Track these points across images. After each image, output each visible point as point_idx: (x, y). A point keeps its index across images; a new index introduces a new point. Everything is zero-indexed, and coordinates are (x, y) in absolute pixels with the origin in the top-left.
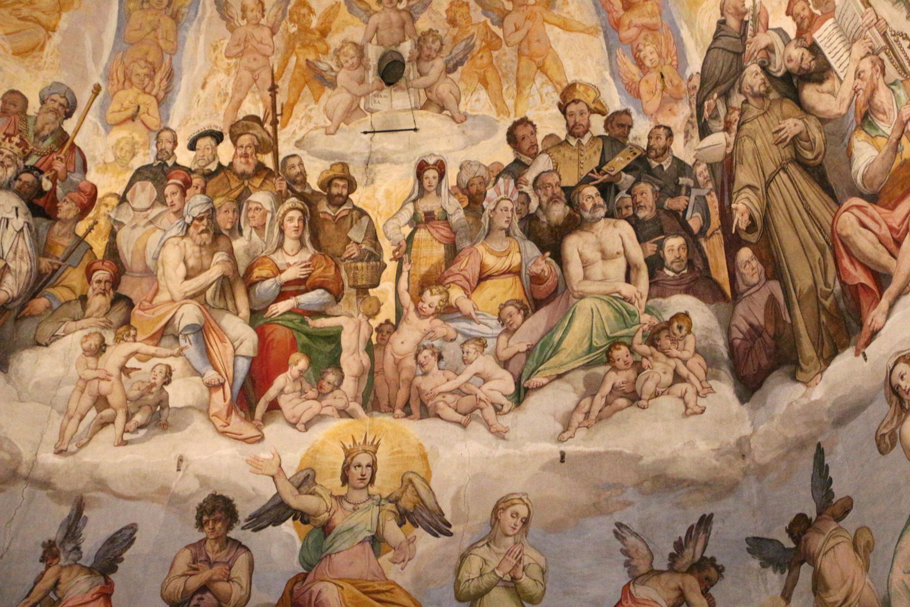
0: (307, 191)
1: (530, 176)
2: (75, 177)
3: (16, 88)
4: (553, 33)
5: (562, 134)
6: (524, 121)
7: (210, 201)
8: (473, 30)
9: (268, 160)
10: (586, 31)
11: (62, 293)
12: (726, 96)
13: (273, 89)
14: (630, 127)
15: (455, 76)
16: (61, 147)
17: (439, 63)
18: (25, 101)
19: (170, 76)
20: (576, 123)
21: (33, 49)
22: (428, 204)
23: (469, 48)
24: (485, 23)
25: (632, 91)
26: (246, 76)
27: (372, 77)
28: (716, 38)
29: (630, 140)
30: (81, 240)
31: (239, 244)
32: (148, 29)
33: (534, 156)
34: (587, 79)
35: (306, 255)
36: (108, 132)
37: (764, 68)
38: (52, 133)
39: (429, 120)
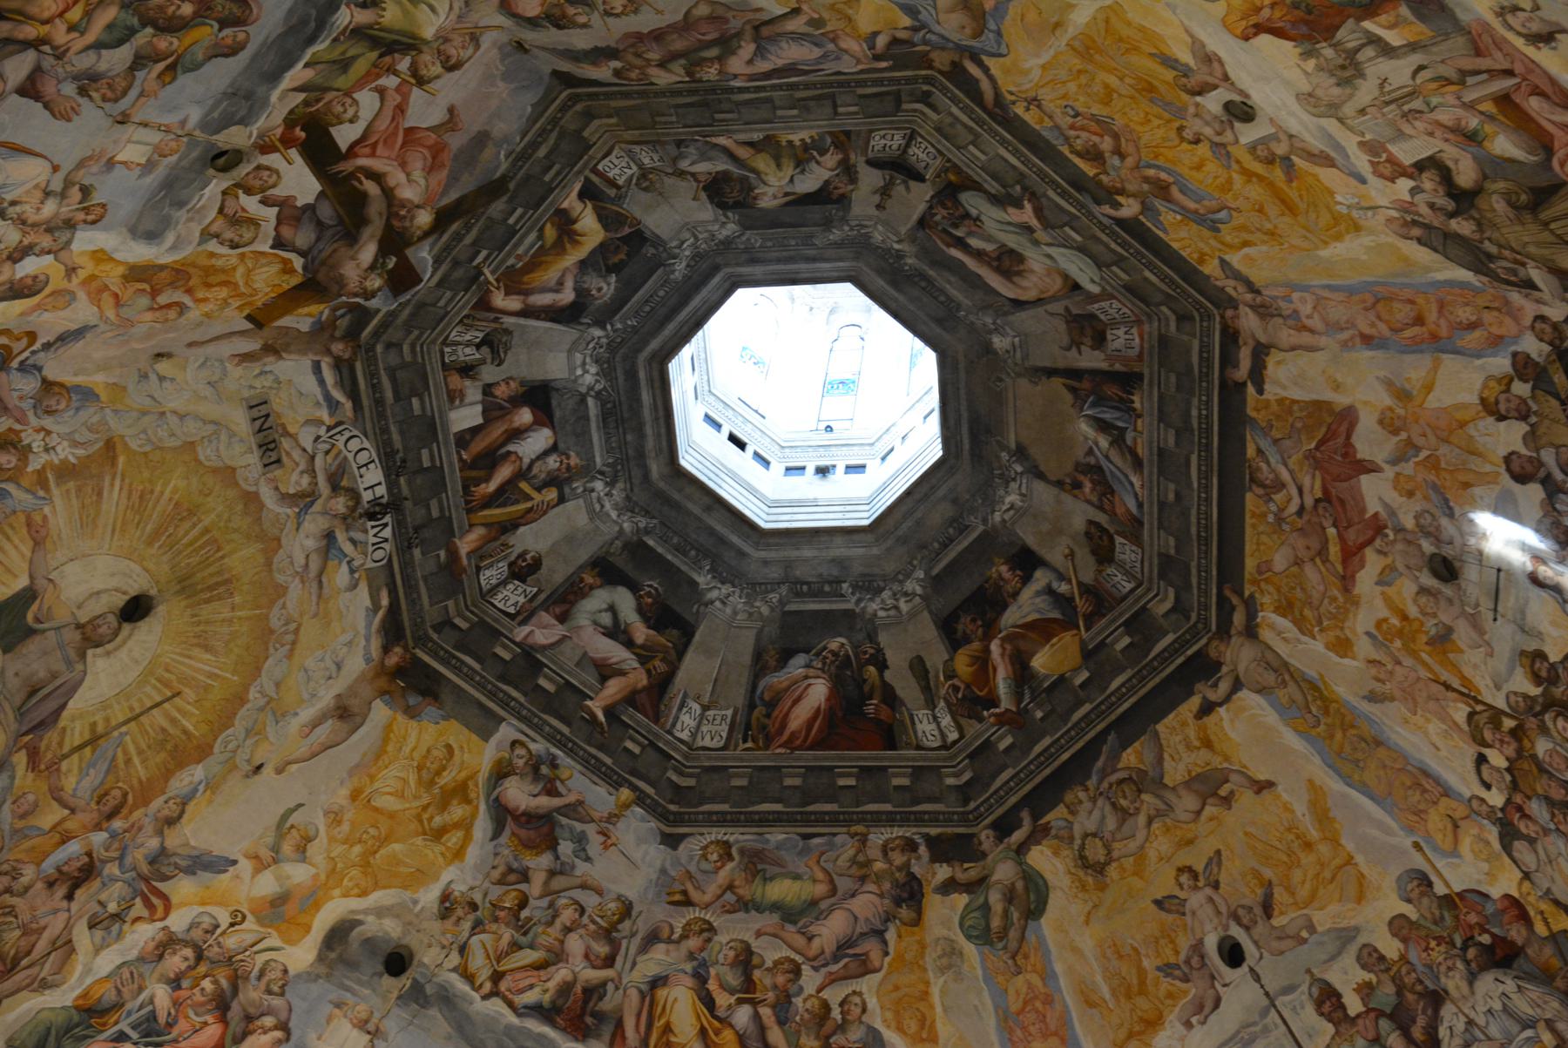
0: (1540, 700)
2: (1490, 909)
3: (1388, 916)
4: (1433, 402)
5: (1523, 428)
6: (1508, 459)
7: (1538, 796)
8: (1419, 478)
9: (1508, 723)
10: (1435, 369)
12: (1490, 257)
13: (1448, 687)
14: (1528, 356)
16: (1455, 906)
17: (1444, 521)
19: (1426, 774)
20: (1517, 410)
21: (1361, 885)
23: (1435, 487)
24: (1417, 464)
25: (1496, 342)
26: (1432, 705)
27: (1447, 590)
28: (1436, 250)
30: (1553, 937)
32: (1382, 773)
33: (1541, 464)
34: (1478, 385)
36: (1459, 856)
37: (1452, 215)
38: (1440, 907)
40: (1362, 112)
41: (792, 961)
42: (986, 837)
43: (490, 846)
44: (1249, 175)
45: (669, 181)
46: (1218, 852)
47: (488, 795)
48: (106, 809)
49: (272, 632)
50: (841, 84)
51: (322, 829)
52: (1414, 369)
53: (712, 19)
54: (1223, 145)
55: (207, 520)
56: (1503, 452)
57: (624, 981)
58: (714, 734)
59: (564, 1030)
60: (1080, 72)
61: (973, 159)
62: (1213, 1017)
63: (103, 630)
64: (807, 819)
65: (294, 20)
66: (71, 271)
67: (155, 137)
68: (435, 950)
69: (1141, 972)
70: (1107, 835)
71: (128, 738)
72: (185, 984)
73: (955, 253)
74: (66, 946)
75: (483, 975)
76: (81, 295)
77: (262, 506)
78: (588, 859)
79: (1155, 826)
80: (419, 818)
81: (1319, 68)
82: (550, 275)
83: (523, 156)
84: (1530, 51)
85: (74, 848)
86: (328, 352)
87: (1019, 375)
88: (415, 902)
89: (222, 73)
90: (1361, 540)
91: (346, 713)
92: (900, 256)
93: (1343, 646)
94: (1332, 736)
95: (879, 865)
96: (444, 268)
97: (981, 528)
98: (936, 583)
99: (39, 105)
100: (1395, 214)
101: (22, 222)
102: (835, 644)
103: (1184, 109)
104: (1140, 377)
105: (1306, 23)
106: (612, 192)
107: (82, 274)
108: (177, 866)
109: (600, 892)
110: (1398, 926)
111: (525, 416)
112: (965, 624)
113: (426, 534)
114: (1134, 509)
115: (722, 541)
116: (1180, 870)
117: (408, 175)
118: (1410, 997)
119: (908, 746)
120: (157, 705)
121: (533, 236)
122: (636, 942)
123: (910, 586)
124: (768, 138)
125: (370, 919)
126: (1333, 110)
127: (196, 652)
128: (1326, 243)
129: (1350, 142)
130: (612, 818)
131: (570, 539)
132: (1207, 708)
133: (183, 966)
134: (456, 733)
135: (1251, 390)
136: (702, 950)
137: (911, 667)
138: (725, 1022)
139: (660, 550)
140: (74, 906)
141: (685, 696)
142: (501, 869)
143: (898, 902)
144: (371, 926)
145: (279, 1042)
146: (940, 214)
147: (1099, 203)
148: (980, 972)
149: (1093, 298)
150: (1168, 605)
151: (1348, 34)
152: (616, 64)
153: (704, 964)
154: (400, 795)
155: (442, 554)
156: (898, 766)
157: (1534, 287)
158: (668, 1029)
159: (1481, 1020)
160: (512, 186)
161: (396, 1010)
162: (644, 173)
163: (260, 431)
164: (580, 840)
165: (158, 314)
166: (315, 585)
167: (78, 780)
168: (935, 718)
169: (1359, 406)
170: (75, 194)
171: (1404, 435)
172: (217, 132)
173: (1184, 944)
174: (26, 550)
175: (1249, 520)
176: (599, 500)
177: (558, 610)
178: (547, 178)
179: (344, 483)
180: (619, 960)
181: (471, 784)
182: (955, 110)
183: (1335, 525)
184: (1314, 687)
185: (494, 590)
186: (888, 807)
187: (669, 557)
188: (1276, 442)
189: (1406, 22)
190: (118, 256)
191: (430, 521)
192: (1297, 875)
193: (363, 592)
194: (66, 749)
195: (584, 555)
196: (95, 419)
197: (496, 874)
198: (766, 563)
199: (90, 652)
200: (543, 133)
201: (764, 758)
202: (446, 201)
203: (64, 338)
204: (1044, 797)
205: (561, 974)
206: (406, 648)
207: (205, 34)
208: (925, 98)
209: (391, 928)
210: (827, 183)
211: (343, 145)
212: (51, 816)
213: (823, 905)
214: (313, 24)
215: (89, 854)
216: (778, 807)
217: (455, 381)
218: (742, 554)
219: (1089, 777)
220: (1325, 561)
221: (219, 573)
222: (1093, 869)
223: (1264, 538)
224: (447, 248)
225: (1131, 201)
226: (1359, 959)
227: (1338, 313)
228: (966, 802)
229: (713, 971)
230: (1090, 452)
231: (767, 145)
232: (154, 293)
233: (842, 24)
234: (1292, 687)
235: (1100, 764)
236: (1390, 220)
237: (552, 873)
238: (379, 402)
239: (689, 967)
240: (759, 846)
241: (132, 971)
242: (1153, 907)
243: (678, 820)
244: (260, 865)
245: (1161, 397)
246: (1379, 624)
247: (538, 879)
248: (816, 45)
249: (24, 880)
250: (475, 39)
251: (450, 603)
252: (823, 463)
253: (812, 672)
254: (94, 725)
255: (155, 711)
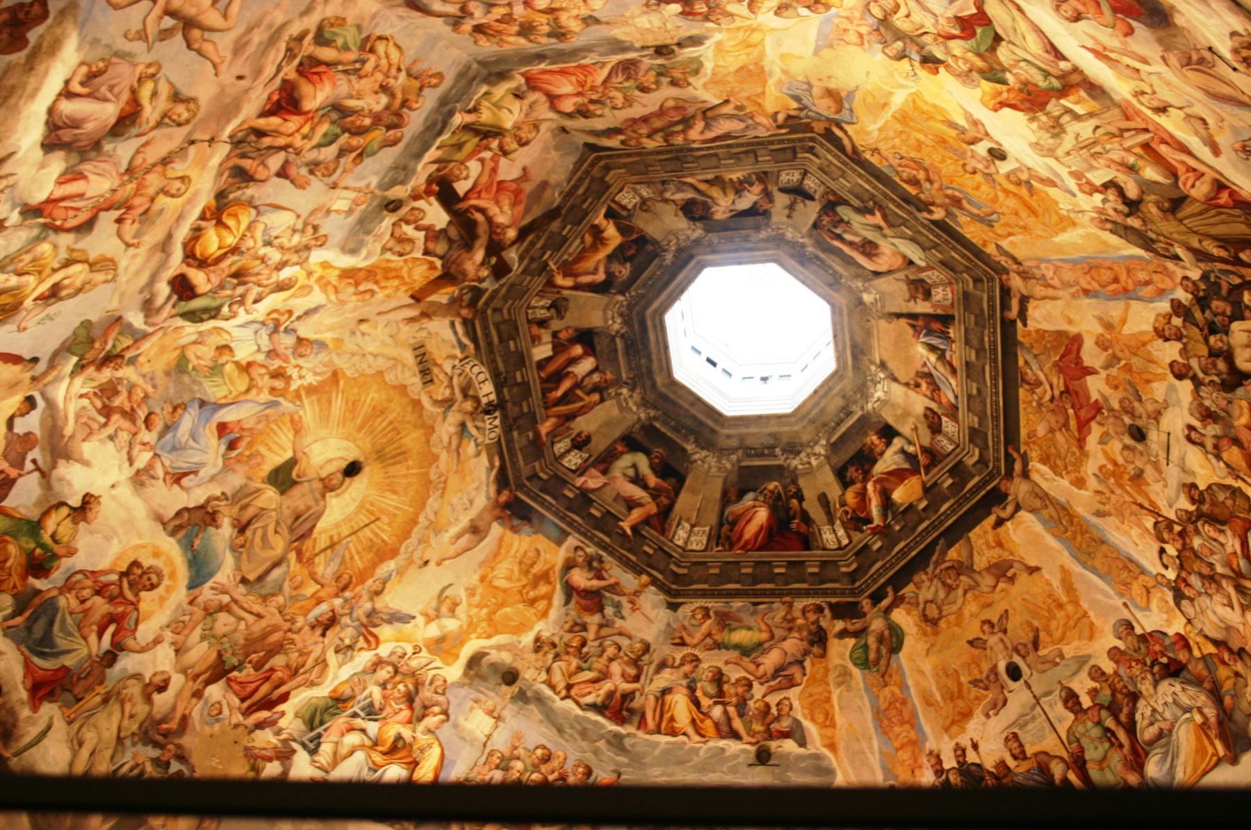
1: (1201, 375)
2: (1167, 642)
3: (1107, 648)
4: (1128, 329)
5: (1178, 346)
6: (1171, 365)
8: (1121, 377)
9: (1177, 528)
10: (1127, 308)
11: (1228, 685)
12: (1152, 240)
13: (1142, 507)
14: (1179, 302)
15: (1144, 398)
17: (1136, 404)
18: (1115, 648)
19: (1131, 560)
22: (1209, 444)
23: (1130, 383)
25: (1161, 293)
26: (1133, 518)
27: (1140, 447)
29: (1186, 303)
30: (1203, 657)
31: (1219, 569)
33: (1190, 368)
34: (1152, 319)
35: (1229, 533)
37: (1128, 215)
39: (1165, 421)
40: (1068, 154)
41: (745, 678)
42: (866, 604)
43: (563, 610)
44: (1006, 192)
45: (659, 205)
46: (1006, 611)
47: (562, 579)
48: (341, 585)
49: (431, 482)
50: (759, 144)
51: (464, 598)
52: (1115, 310)
53: (677, 108)
54: (990, 175)
55: (392, 416)
56: (1168, 360)
57: (646, 690)
58: (698, 542)
59: (609, 719)
60: (901, 132)
61: (843, 186)
62: (1003, 711)
63: (335, 482)
64: (756, 593)
65: (429, 123)
66: (310, 274)
67: (352, 195)
68: (532, 671)
69: (960, 685)
70: (939, 601)
71: (351, 545)
72: (389, 686)
73: (837, 243)
74: (323, 663)
75: (561, 687)
76: (316, 288)
77: (422, 408)
78: (622, 618)
79: (969, 595)
80: (520, 592)
81: (1040, 128)
82: (590, 264)
83: (569, 194)
84: (1155, 117)
85: (324, 607)
86: (459, 315)
87: (880, 318)
88: (520, 642)
89: (388, 156)
90: (1089, 416)
91: (476, 530)
92: (803, 246)
93: (1080, 483)
94: (1075, 539)
95: (800, 621)
96: (525, 262)
97: (859, 413)
98: (834, 447)
99: (287, 182)
100: (1095, 215)
101: (281, 248)
102: (772, 485)
103: (965, 152)
104: (952, 317)
105: (1029, 101)
106: (624, 213)
107: (316, 276)
108: (382, 619)
109: (630, 637)
110: (1114, 654)
111: (578, 350)
112: (852, 472)
113: (521, 422)
114: (953, 400)
115: (701, 423)
116: (984, 622)
117: (501, 208)
118: (1119, 696)
119: (818, 548)
120: (367, 525)
121: (578, 241)
122: (652, 668)
123: (819, 449)
124: (717, 177)
125: (493, 652)
126: (1051, 152)
127: (388, 494)
128: (1057, 234)
129: (1063, 172)
130: (637, 593)
131: (608, 424)
132: (1000, 523)
133: (388, 676)
134: (541, 542)
135: (1019, 324)
136: (692, 672)
137: (819, 499)
138: (707, 715)
139: (663, 430)
140: (326, 640)
141: (681, 519)
142: (570, 623)
143: (812, 643)
144: (494, 656)
145: (443, 721)
146: (826, 220)
147: (920, 210)
148: (862, 685)
149: (921, 269)
150: (976, 458)
151: (1053, 107)
152: (621, 137)
153: (694, 681)
154: (509, 579)
155: (531, 434)
156: (811, 558)
157: (1180, 259)
158: (672, 719)
159: (1160, 709)
160: (563, 212)
161: (510, 706)
162: (644, 202)
163: (421, 363)
164: (618, 606)
165: (360, 297)
166: (455, 454)
167: (325, 568)
168: (834, 531)
169: (1084, 333)
170: (310, 230)
171: (1110, 351)
172: (387, 189)
173: (986, 667)
174: (291, 436)
175: (1022, 406)
176: (625, 400)
177: (602, 467)
178: (585, 206)
179: (471, 393)
180: (643, 678)
181: (551, 573)
182: (829, 157)
183: (1073, 407)
184: (1064, 508)
185: (563, 455)
186: (805, 586)
187: (669, 434)
188: (1035, 356)
189: (1085, 100)
190: (335, 264)
191: (522, 415)
192: (1054, 624)
193: (484, 459)
194: (317, 550)
195: (617, 433)
196: (326, 359)
197: (567, 626)
198: (729, 436)
199: (328, 495)
200: (581, 180)
201: (729, 557)
202: (524, 223)
203: (308, 313)
204: (901, 578)
205: (607, 686)
206: (511, 491)
207: (379, 134)
208: (811, 150)
209: (506, 658)
210: (755, 203)
211: (461, 192)
212: (311, 589)
213: (766, 645)
214: (440, 125)
215: (333, 611)
216: (738, 586)
217: (535, 330)
218: (713, 431)
219: (928, 566)
220: (1068, 430)
221: (400, 447)
222: (931, 622)
223: (1031, 416)
224: (527, 251)
225: (939, 209)
226: (1090, 674)
227: (1068, 276)
228: (853, 582)
229: (699, 685)
230: (925, 365)
231: (717, 182)
232: (357, 284)
233: (756, 108)
234: (1051, 510)
235: (934, 558)
236: (1092, 219)
237: (601, 626)
238: (490, 344)
239: (684, 682)
240: (726, 610)
241: (359, 679)
242: (967, 646)
243: (677, 594)
244: (429, 619)
245: (966, 330)
246: (1101, 468)
247: (592, 630)
248: (742, 121)
249: (298, 625)
250: (536, 127)
251: (537, 464)
252: (764, 375)
253: (757, 503)
254: (331, 537)
255: (366, 529)
